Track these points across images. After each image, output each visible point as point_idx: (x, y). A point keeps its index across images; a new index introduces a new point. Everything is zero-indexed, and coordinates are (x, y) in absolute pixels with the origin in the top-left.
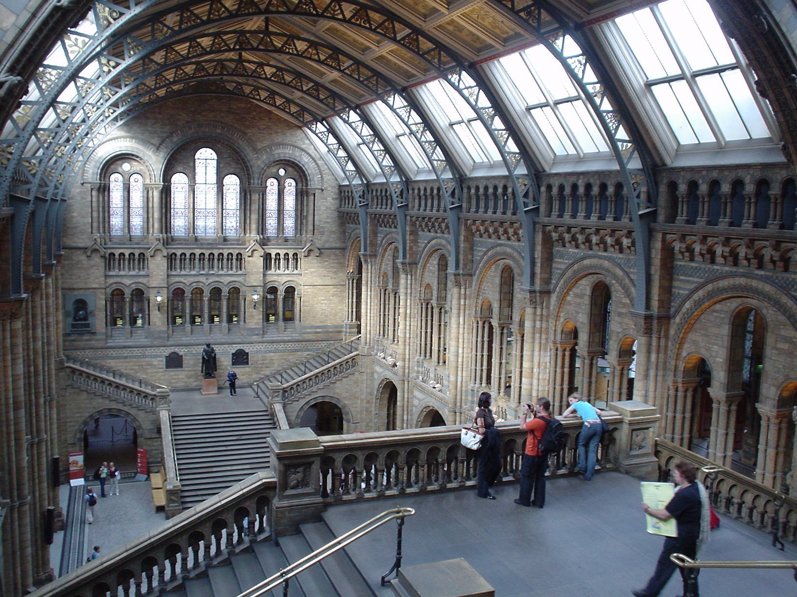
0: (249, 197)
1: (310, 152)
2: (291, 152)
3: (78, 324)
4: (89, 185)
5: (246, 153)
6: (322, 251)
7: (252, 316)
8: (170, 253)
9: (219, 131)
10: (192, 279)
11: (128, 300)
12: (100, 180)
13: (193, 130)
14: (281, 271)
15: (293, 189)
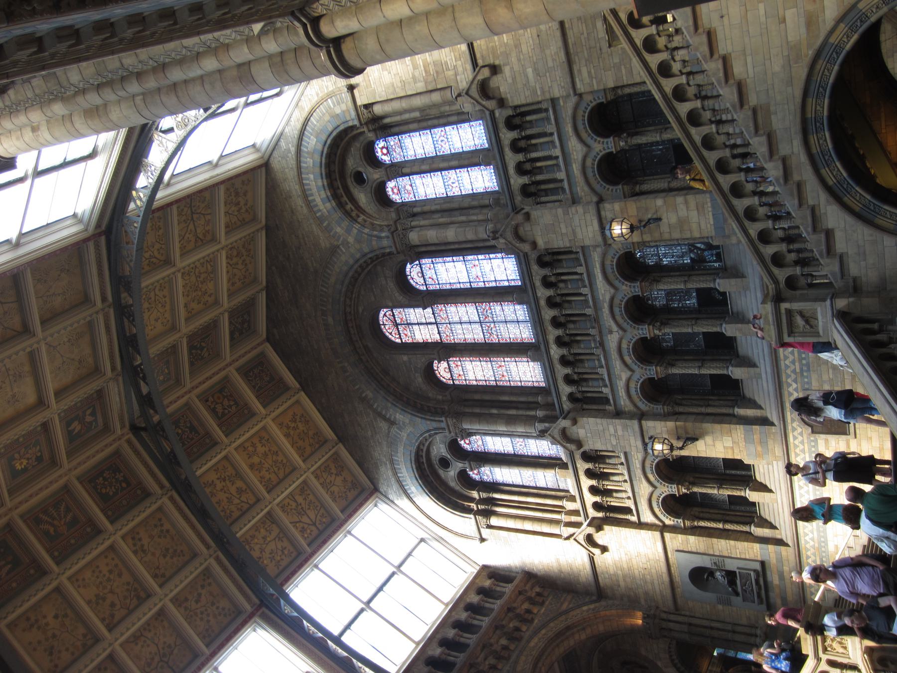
0: (423, 249)
1: (296, 133)
2: (312, 176)
3: (744, 591)
4: (482, 530)
5: (345, 268)
6: (478, 55)
7: (682, 223)
8: (568, 403)
9: (330, 320)
10: (617, 365)
11: (684, 491)
12: (468, 510)
13: (346, 364)
14: (557, 152)
15: (392, 141)
